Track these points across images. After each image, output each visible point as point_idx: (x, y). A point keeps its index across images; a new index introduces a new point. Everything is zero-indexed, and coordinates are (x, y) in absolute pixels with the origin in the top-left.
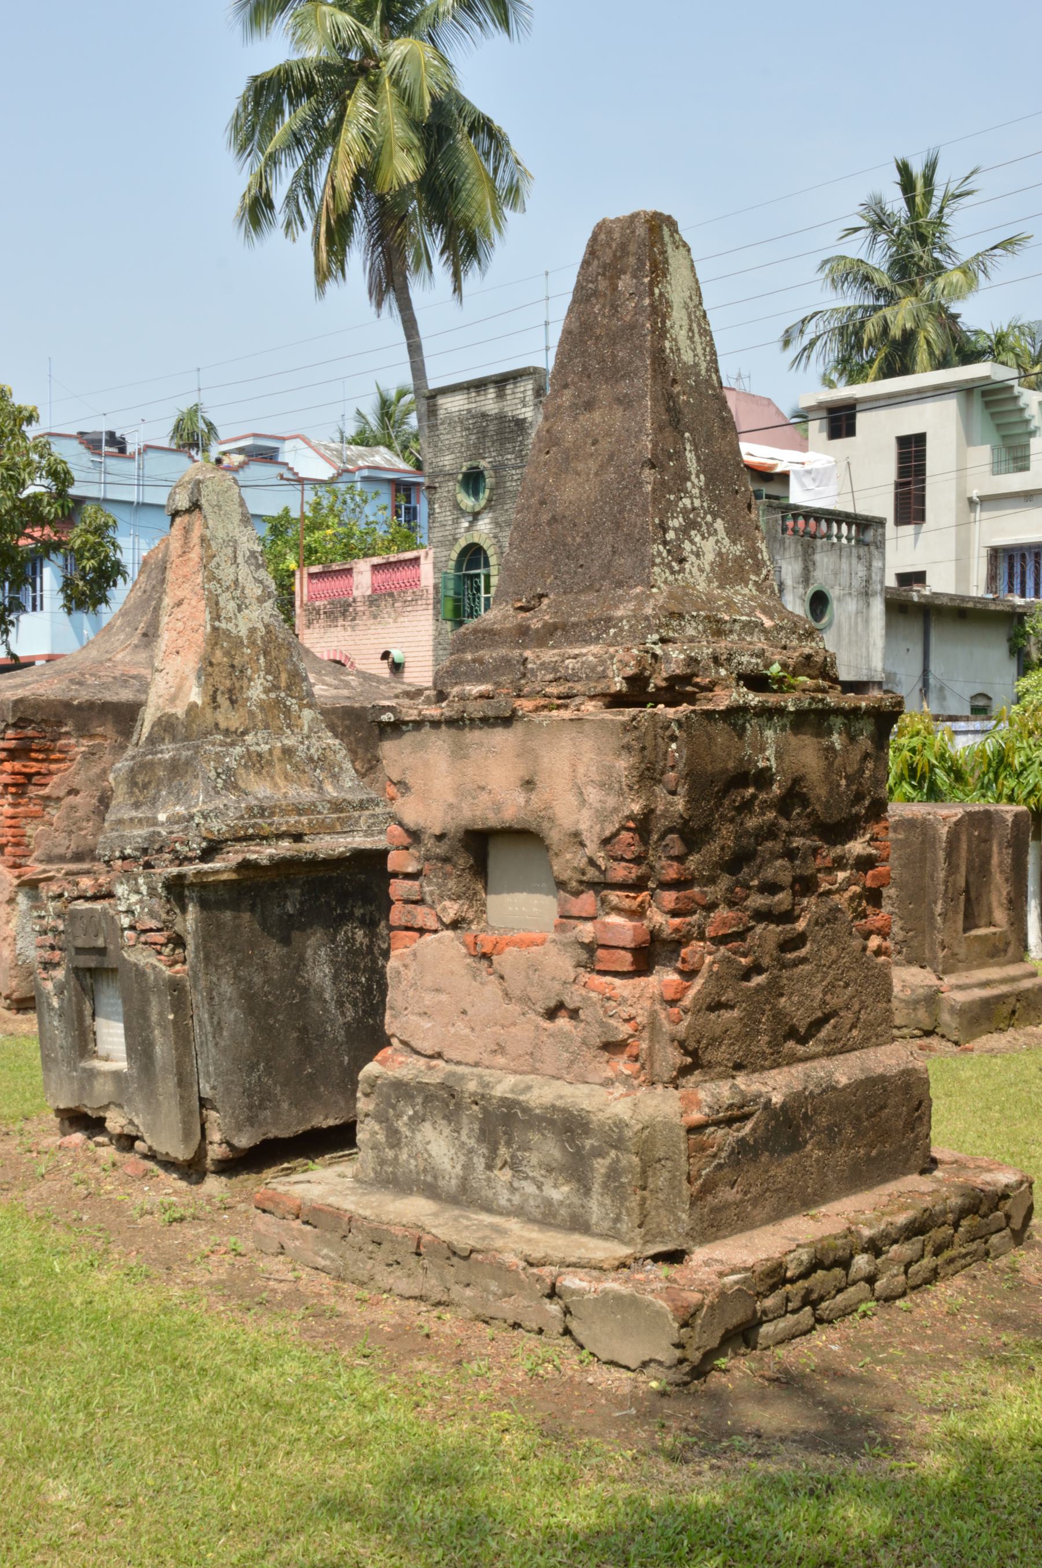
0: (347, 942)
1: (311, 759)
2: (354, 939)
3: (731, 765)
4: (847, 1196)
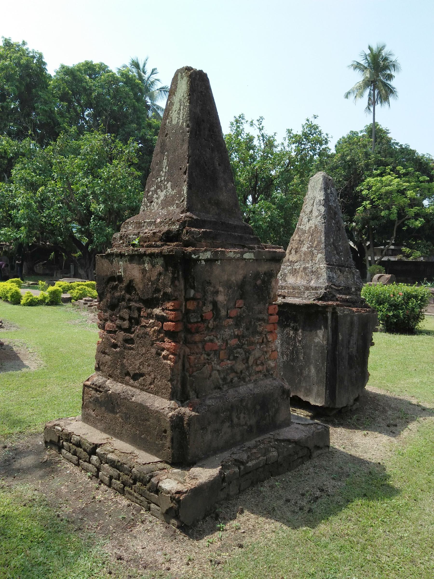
0: (287, 334)
1: (312, 272)
2: (289, 334)
3: (109, 274)
4: (130, 444)
